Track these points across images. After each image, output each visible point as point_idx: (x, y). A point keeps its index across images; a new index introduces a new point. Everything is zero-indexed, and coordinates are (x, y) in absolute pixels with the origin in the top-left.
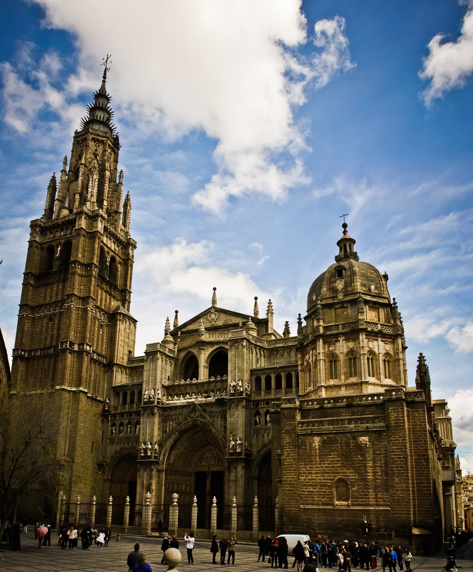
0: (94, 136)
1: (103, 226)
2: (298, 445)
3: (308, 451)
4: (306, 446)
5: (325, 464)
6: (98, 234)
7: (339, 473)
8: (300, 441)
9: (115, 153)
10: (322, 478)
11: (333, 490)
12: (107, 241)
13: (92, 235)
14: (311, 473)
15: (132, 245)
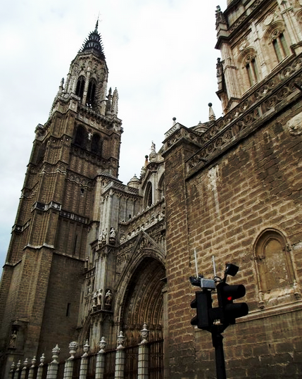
1: (76, 106)
3: (202, 203)
4: (197, 195)
5: (230, 214)
7: (260, 221)
8: (189, 191)
9: (101, 64)
10: (228, 246)
11: (252, 268)
14: (209, 245)
15: (116, 122)
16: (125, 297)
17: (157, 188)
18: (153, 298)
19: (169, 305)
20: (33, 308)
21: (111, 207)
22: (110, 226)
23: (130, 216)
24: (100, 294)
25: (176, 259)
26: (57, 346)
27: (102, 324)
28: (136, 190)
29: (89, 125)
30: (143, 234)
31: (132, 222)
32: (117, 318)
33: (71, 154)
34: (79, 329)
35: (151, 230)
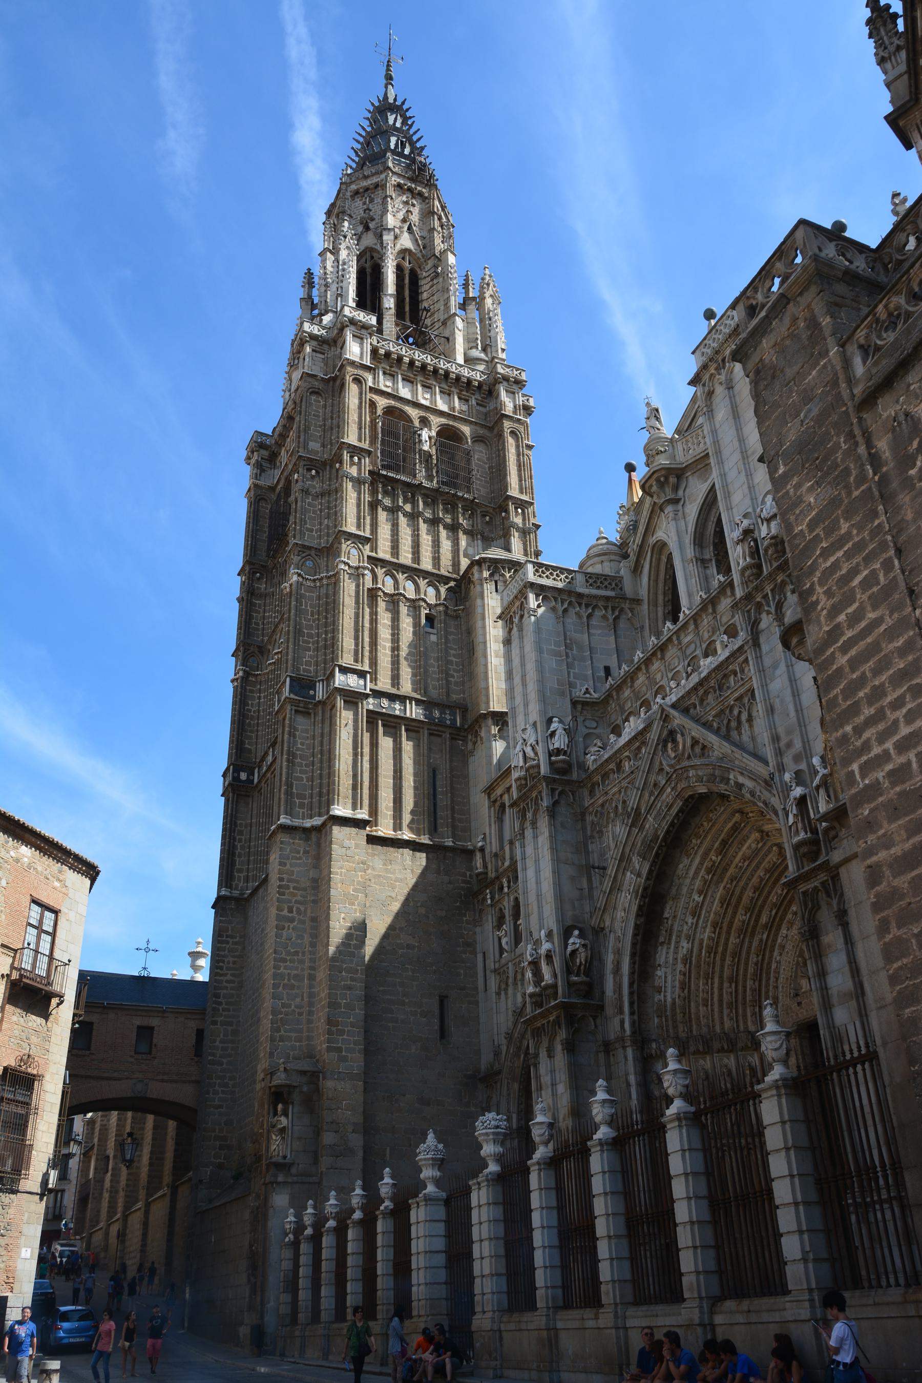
0: (354, 187)
1: (368, 348)
2: (884, 482)
6: (349, 369)
8: (883, 445)
12: (414, 392)
13: (338, 382)
15: (506, 379)
16: (634, 945)
17: (690, 552)
18: (733, 940)
19: (877, 907)
20: (329, 1022)
21: (540, 650)
22: (543, 712)
23: (607, 670)
24: (546, 946)
25: (880, 715)
26: (431, 1137)
27: (570, 1048)
28: (613, 581)
29: (417, 405)
30: (666, 718)
31: (619, 688)
32: (619, 1023)
33: (374, 506)
34: (489, 1079)
35: (694, 699)
